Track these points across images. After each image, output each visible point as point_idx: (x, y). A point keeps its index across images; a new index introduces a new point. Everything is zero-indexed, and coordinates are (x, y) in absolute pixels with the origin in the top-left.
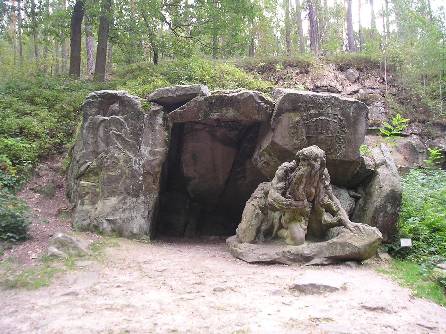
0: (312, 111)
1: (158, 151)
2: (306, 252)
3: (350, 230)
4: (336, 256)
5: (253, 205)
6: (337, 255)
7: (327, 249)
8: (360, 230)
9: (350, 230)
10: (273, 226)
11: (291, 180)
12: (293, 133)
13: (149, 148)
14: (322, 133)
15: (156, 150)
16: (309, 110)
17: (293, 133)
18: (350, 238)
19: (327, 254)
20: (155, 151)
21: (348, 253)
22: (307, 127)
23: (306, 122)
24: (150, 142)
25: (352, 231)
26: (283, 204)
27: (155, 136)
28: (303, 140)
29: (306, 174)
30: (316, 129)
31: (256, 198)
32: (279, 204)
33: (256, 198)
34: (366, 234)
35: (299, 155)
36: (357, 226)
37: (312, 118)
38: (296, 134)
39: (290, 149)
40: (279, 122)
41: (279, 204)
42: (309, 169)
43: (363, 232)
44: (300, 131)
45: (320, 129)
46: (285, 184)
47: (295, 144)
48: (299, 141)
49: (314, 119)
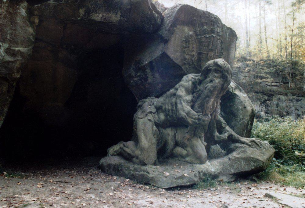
0: (205, 27)
1: (19, 51)
2: (213, 170)
3: (247, 144)
4: (241, 172)
5: (150, 120)
6: (243, 171)
7: (232, 166)
8: (258, 145)
9: (247, 144)
10: (166, 144)
11: (200, 92)
12: (185, 48)
13: (6, 45)
14: (212, 50)
15: (17, 49)
16: (203, 26)
17: (185, 48)
18: (252, 153)
19: (232, 171)
20: (14, 50)
21: (253, 168)
22: (200, 42)
23: (199, 37)
24: (8, 37)
25: (250, 146)
26: (194, 119)
27: (15, 30)
28: (193, 56)
29: (219, 86)
30: (208, 46)
31: (151, 113)
32: (192, 118)
33: (151, 113)
34: (264, 148)
35: (209, 66)
36: (254, 141)
37: (205, 34)
38: (187, 49)
39: (180, 64)
40: (173, 33)
41: (192, 118)
42: (222, 82)
43: (261, 147)
44: (191, 46)
45: (211, 47)
46: (193, 97)
47: (185, 59)
48: (189, 57)
49: (208, 36)
